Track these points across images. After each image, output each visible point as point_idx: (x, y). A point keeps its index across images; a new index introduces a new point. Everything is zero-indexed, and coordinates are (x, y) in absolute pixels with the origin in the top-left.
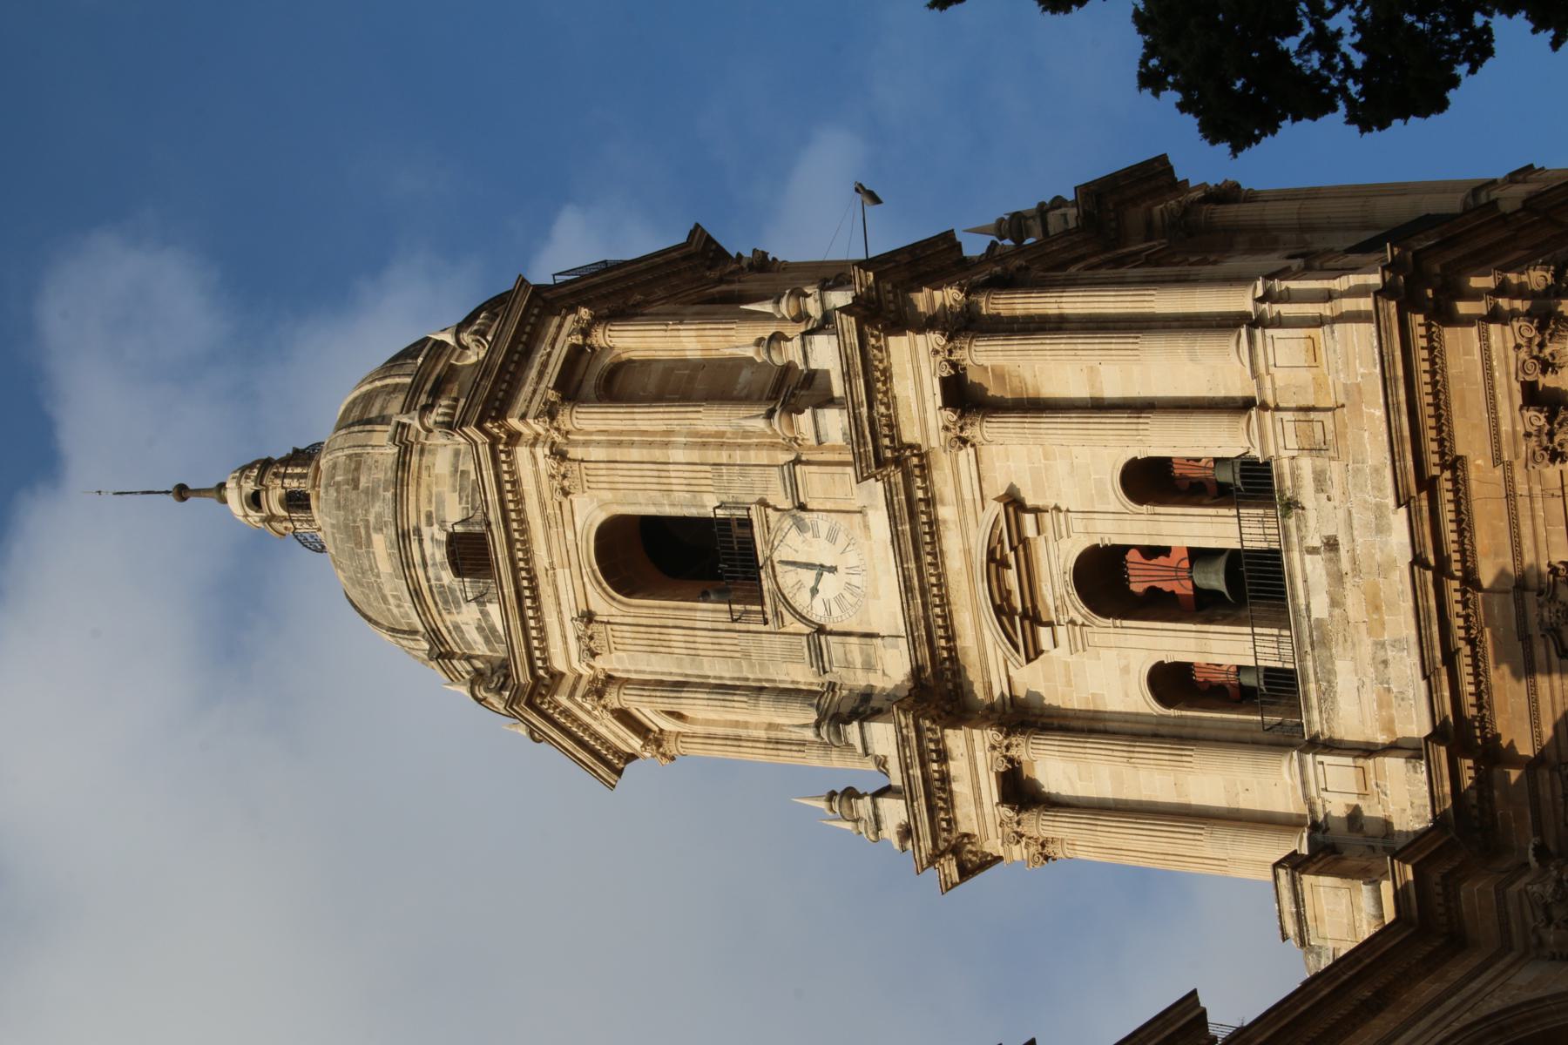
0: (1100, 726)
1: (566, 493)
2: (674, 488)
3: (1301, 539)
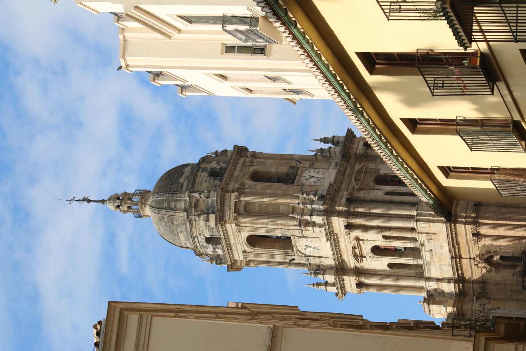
1: (240, 232)
3: (425, 250)
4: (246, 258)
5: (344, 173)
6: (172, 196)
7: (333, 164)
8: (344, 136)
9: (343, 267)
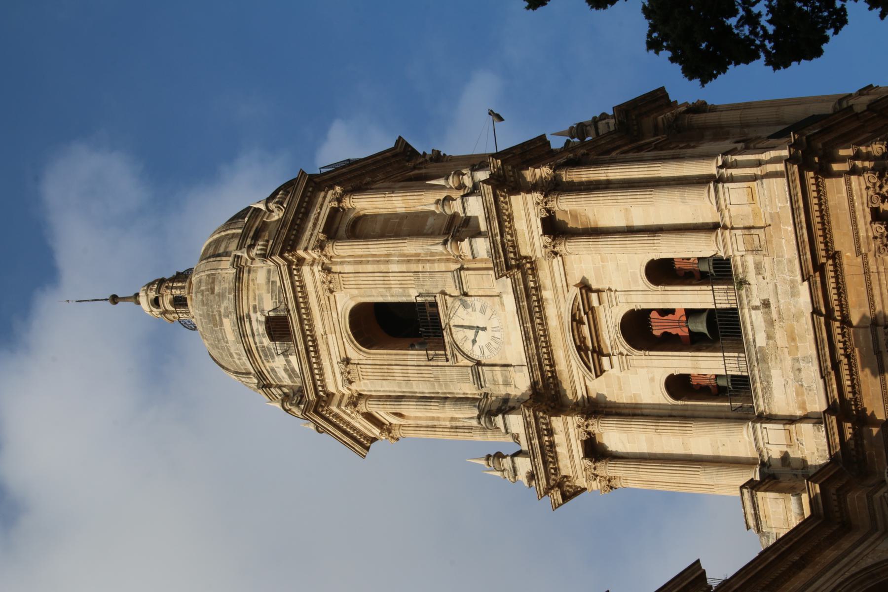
0: (639, 412)
1: (331, 291)
2: (393, 286)
3: (749, 302)
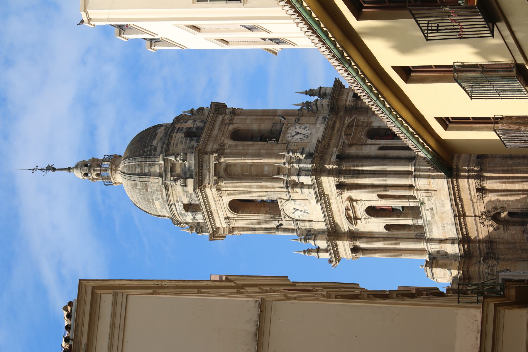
1: (221, 197)
4: (229, 225)
5: (333, 128)
6: (145, 160)
7: (321, 118)
8: (331, 88)
9: (335, 231)
